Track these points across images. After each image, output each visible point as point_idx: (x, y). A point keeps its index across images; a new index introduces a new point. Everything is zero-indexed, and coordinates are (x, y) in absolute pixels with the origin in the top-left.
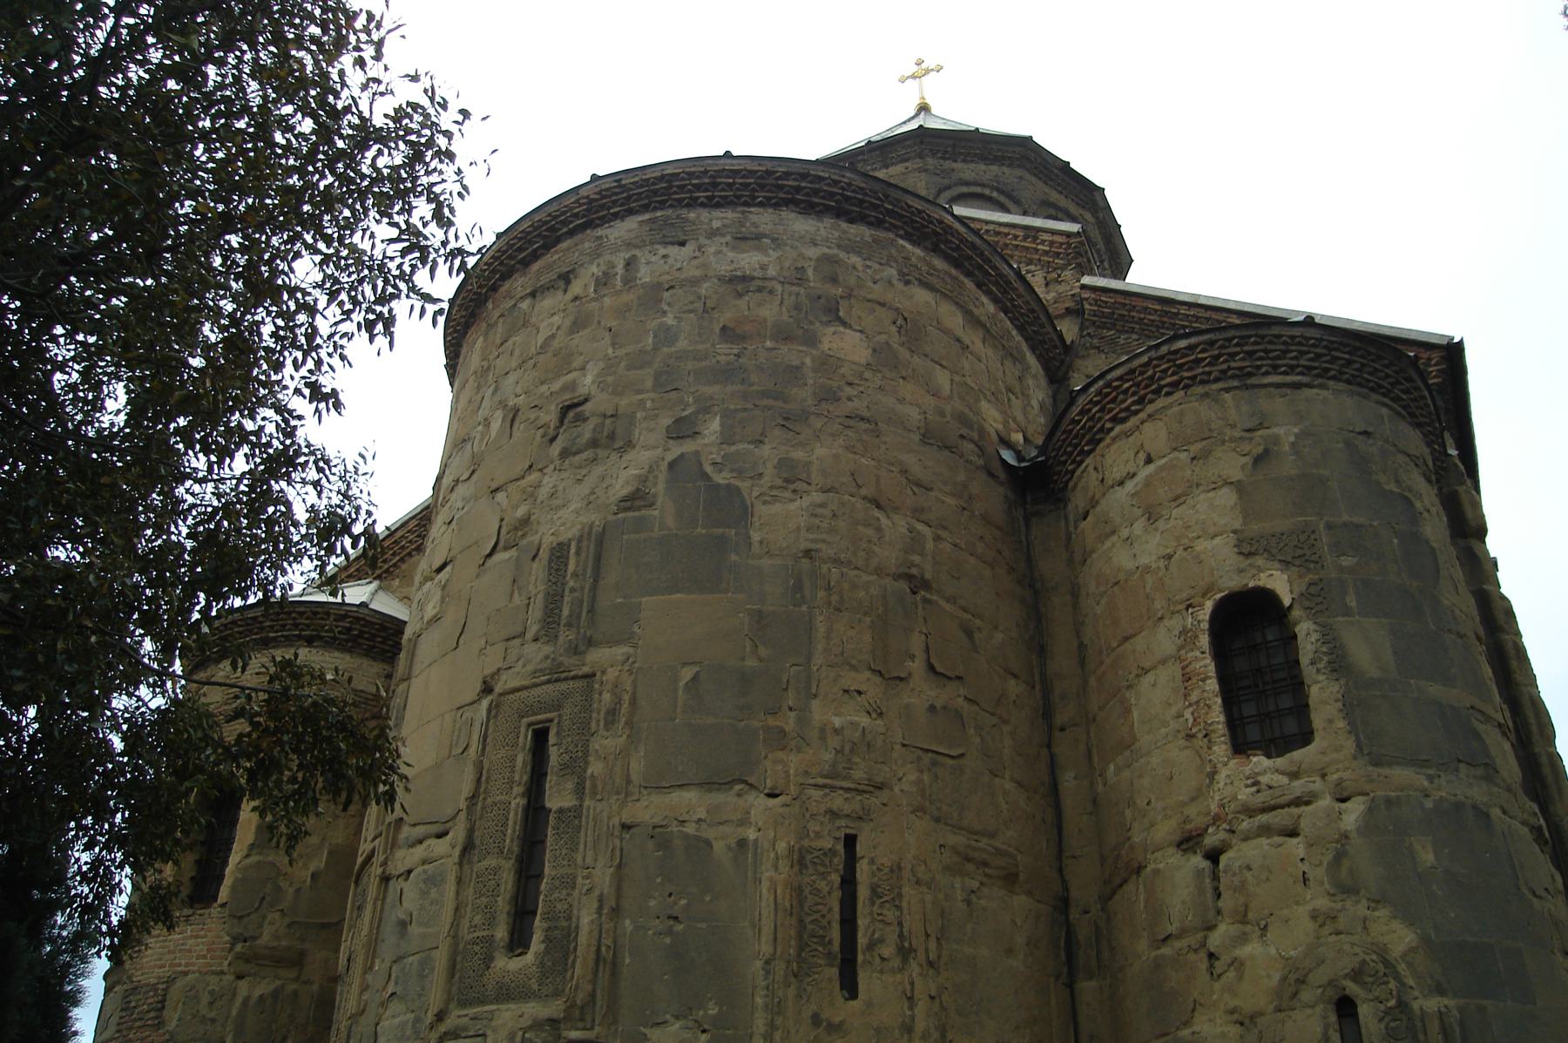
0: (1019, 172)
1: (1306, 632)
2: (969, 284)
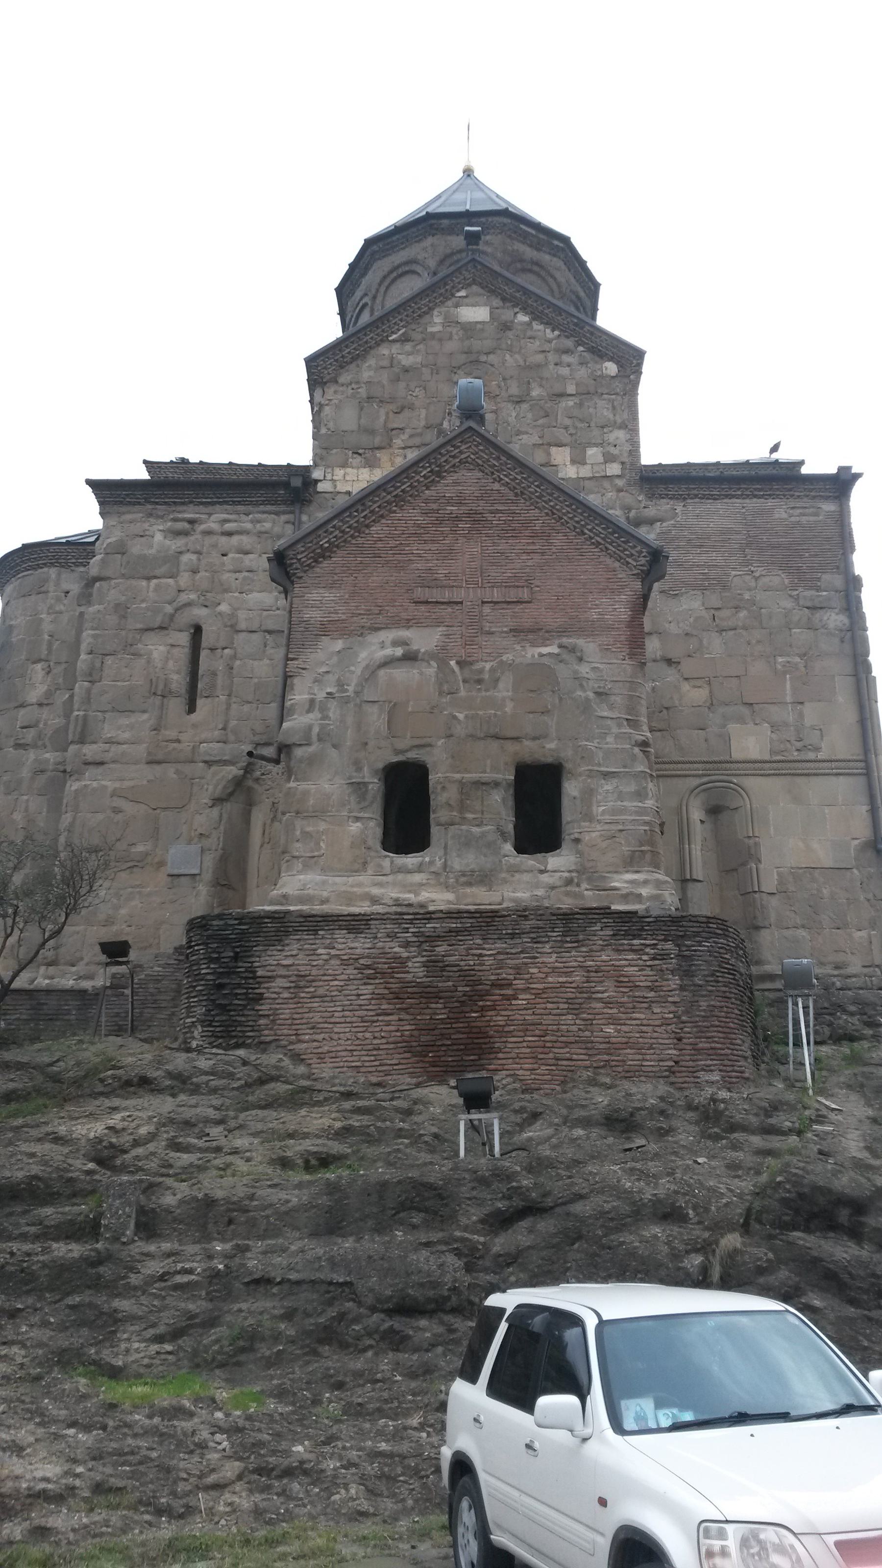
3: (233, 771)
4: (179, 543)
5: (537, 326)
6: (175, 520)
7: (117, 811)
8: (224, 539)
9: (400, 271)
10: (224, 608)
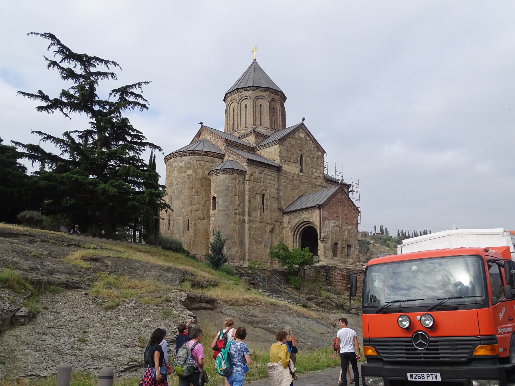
0: (252, 92)
2: (206, 157)
3: (272, 226)
4: (260, 175)
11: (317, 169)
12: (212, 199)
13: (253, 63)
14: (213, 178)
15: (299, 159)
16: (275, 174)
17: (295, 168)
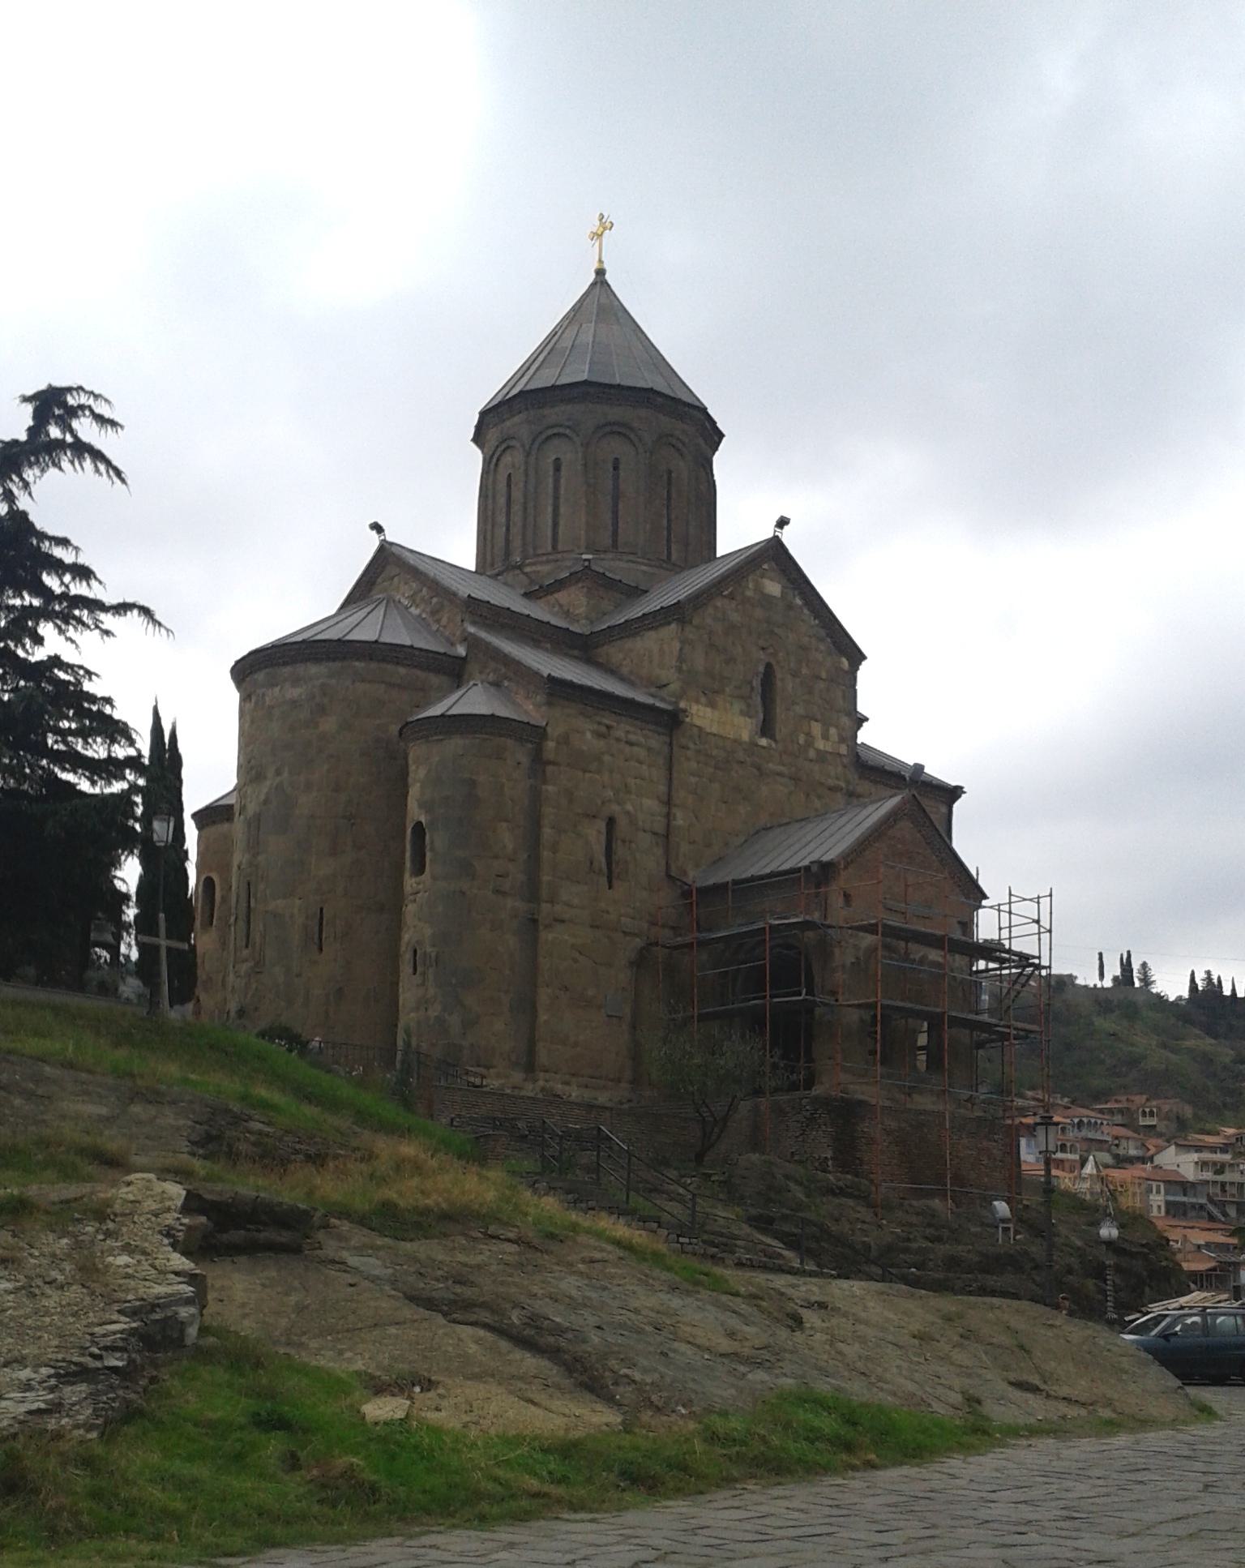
1: (427, 837)
2: (390, 667)
5: (806, 611)
6: (599, 723)
7: (575, 961)
8: (628, 749)
9: (616, 428)
10: (629, 807)
11: (826, 726)
12: (409, 831)
13: (593, 285)
14: (416, 751)
15: (757, 683)
16: (656, 742)
17: (741, 721)
